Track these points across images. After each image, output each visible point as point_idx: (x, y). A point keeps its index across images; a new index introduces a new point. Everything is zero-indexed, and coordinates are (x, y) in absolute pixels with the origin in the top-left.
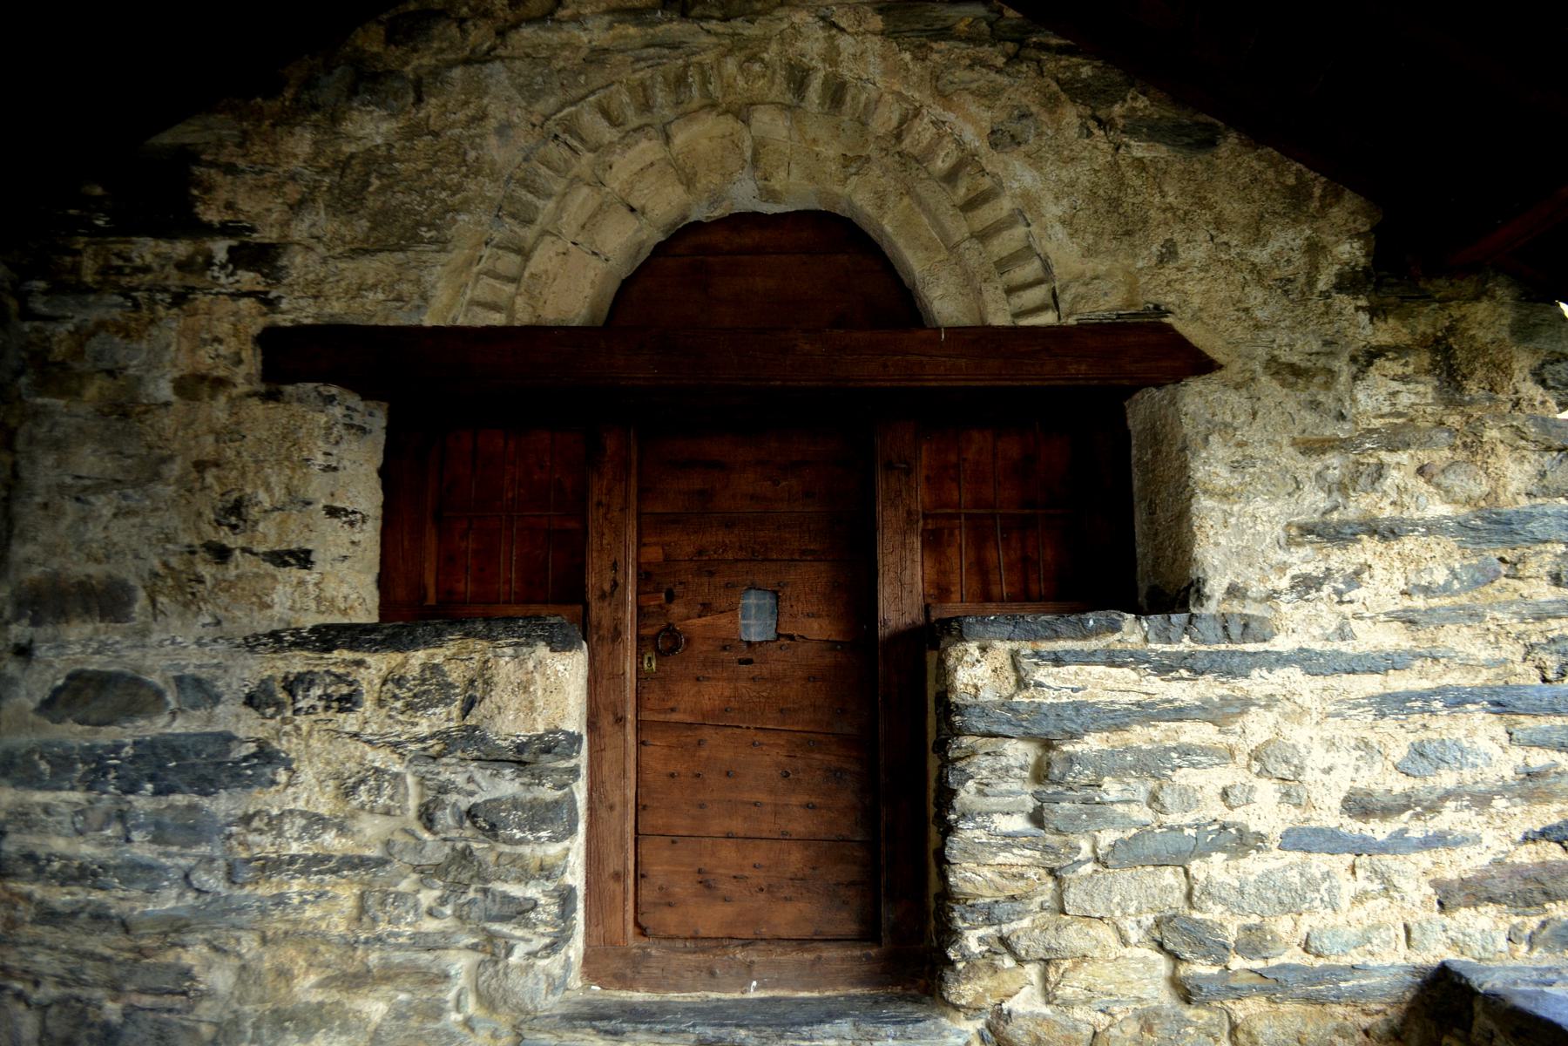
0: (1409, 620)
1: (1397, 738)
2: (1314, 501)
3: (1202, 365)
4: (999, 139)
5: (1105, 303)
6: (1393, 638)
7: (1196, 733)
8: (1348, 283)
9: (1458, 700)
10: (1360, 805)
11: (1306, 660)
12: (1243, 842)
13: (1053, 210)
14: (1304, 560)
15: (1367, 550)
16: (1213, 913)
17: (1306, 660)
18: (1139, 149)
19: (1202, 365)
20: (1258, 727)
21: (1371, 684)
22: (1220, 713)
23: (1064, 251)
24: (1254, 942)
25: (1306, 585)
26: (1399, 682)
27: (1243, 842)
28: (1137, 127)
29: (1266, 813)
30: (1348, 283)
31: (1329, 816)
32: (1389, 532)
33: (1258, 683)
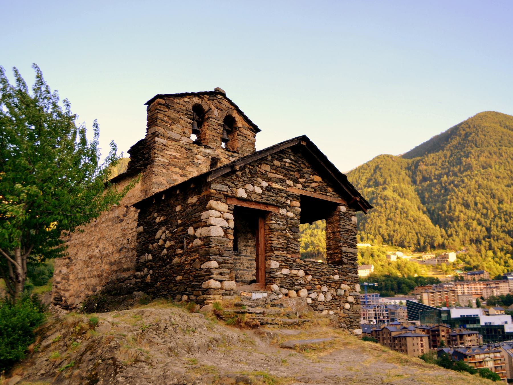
0: (250, 253)
1: (249, 262)
6: (249, 255)
7: (238, 261)
10: (247, 267)
11: (244, 255)
12: (240, 270)
14: (244, 248)
15: (248, 248)
16: (238, 275)
20: (241, 261)
21: (248, 258)
22: (239, 259)
24: (241, 278)
25: (244, 250)
26: (250, 258)
27: (240, 270)
29: (241, 268)
31: (245, 268)
32: (249, 246)
33: (242, 257)
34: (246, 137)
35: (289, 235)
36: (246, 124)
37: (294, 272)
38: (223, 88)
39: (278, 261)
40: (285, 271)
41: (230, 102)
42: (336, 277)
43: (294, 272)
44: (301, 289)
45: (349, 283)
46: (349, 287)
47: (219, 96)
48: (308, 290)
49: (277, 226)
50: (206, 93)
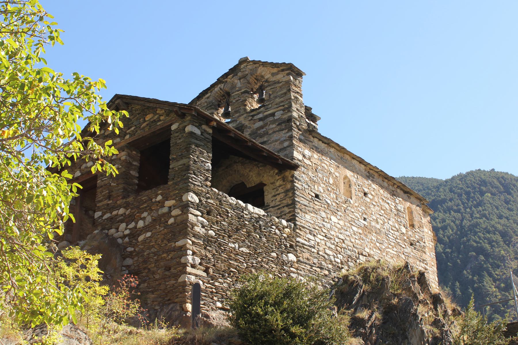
1: (279, 211)
2: (273, 194)
3: (265, 185)
4: (250, 171)
5: (258, 182)
6: (279, 203)
8: (276, 174)
9: (283, 207)
11: (272, 207)
13: (254, 176)
17: (272, 207)
18: (261, 168)
19: (265, 185)
21: (277, 208)
23: (255, 179)
26: (279, 207)
28: (261, 166)
30: (276, 174)
34: (275, 83)
35: (112, 184)
36: (275, 70)
37: (115, 213)
38: (243, 56)
39: (100, 211)
40: (107, 216)
41: (254, 62)
42: (159, 198)
43: (115, 213)
44: (120, 225)
45: (174, 197)
46: (174, 201)
47: (242, 66)
48: (127, 223)
49: (103, 183)
50: (226, 75)
